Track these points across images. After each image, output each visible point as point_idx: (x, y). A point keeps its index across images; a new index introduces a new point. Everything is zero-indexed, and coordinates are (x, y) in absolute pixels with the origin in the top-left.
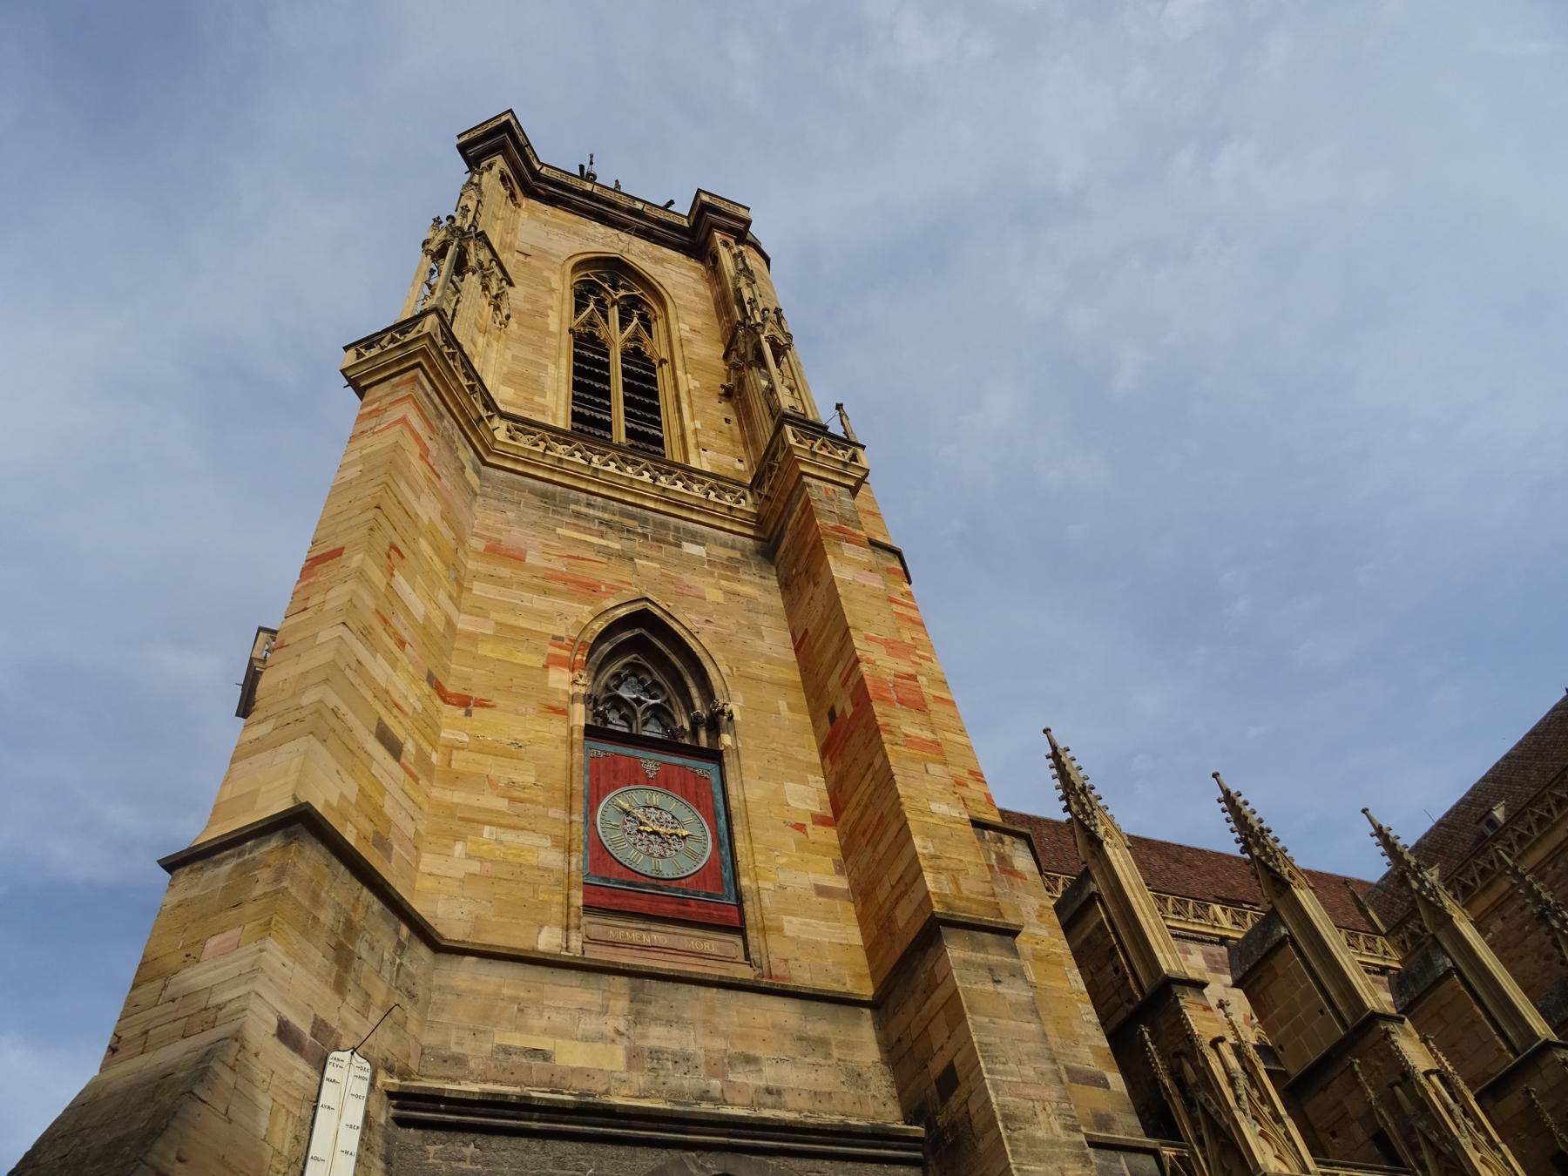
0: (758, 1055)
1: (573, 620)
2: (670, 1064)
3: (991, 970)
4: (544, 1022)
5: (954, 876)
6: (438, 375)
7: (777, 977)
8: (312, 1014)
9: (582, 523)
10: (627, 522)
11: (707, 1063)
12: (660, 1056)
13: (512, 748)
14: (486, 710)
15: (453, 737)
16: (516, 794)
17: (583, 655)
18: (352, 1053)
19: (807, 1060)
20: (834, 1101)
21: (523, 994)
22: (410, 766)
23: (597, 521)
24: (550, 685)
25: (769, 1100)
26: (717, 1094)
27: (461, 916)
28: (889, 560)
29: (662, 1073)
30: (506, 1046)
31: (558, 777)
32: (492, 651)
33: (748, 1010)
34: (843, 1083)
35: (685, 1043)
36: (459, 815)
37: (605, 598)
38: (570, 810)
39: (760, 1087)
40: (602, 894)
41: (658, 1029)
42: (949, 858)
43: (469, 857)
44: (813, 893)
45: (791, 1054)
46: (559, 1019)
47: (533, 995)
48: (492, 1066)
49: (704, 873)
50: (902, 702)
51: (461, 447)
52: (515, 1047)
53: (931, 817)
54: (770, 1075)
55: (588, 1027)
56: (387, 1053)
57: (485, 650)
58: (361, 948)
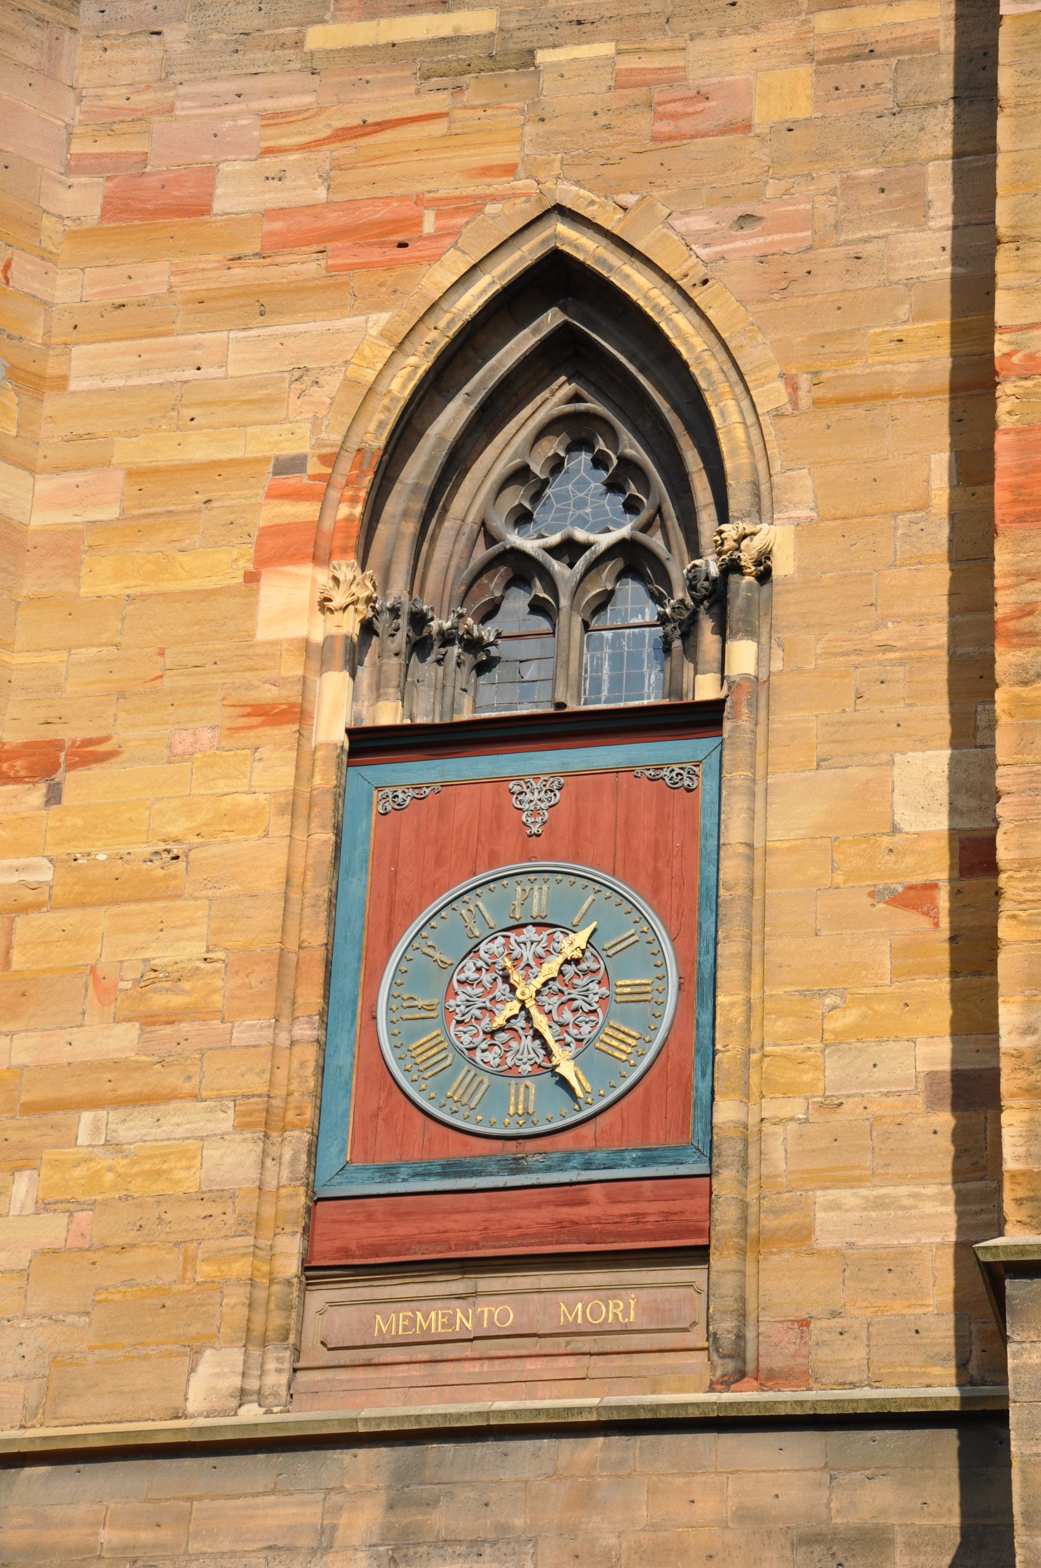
1: (333, 383)
13: (156, 869)
14: (97, 770)
15: (15, 878)
16: (161, 1001)
17: (353, 501)
24: (262, 634)
33: (680, 1481)
36: (25, 1098)
40: (370, 1217)
43: (44, 1206)
49: (647, 1091)
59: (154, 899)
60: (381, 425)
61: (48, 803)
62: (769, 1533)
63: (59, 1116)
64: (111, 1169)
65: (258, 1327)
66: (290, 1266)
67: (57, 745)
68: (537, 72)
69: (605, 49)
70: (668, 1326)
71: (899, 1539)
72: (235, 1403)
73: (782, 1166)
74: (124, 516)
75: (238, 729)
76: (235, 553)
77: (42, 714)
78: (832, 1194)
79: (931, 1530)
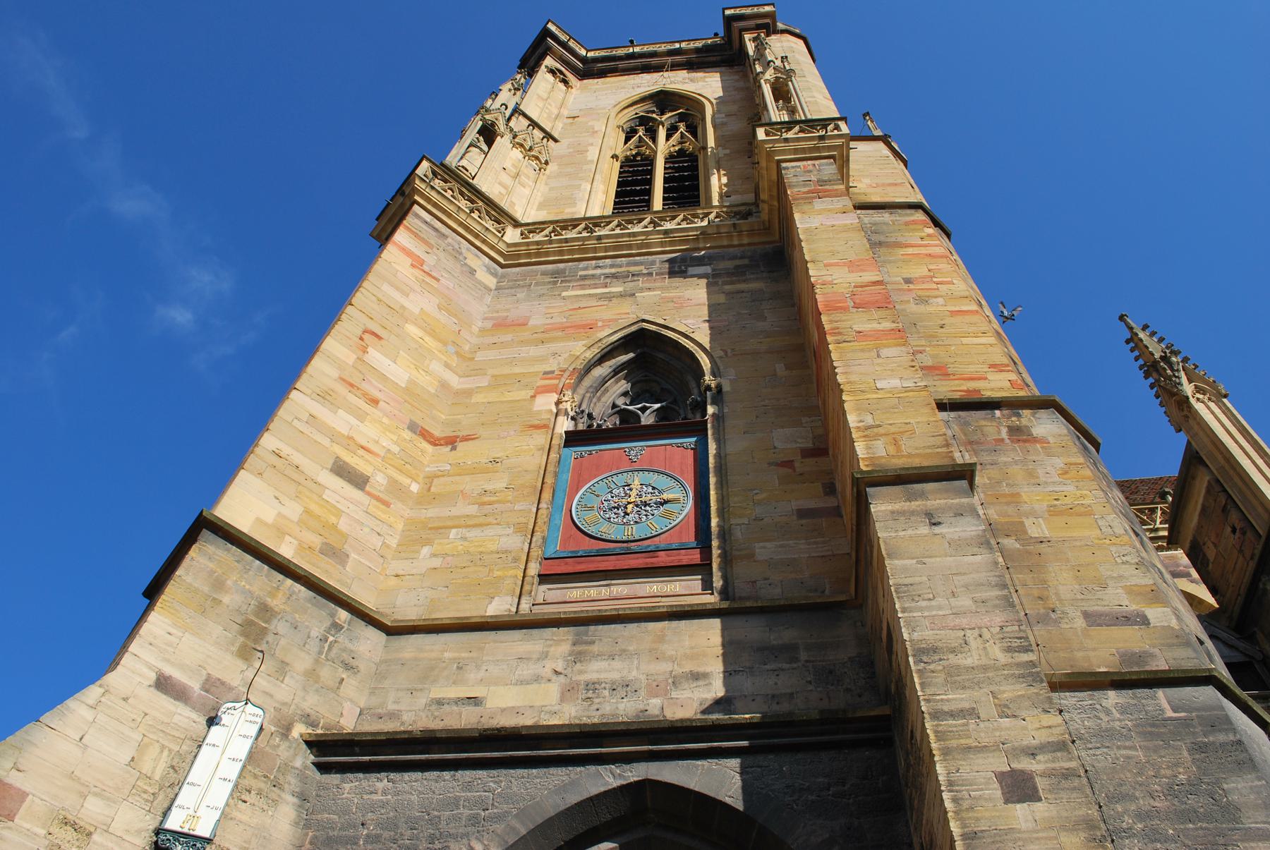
0: (708, 669)
2: (606, 693)
3: (929, 515)
4: (482, 674)
5: (894, 439)
6: (435, 205)
7: (741, 599)
8: (204, 673)
9: (587, 282)
10: (632, 269)
11: (648, 685)
12: (597, 686)
14: (470, 442)
16: (486, 499)
18: (246, 704)
19: (767, 667)
22: (382, 496)
23: (603, 277)
28: (912, 214)
34: (810, 682)
36: (430, 526)
37: (600, 331)
39: (707, 699)
41: (599, 664)
44: (795, 518)
47: (473, 654)
48: (424, 717)
49: (681, 528)
50: (856, 306)
51: (469, 256)
52: (449, 699)
55: (525, 672)
56: (308, 711)
57: (478, 398)
58: (280, 626)
60: (582, 363)
61: (451, 450)
63: (443, 531)
66: (534, 569)
67: (457, 437)
69: (660, 292)
70: (693, 592)
73: (741, 537)
74: (489, 385)
76: (528, 391)
77: (452, 429)
78: (761, 544)
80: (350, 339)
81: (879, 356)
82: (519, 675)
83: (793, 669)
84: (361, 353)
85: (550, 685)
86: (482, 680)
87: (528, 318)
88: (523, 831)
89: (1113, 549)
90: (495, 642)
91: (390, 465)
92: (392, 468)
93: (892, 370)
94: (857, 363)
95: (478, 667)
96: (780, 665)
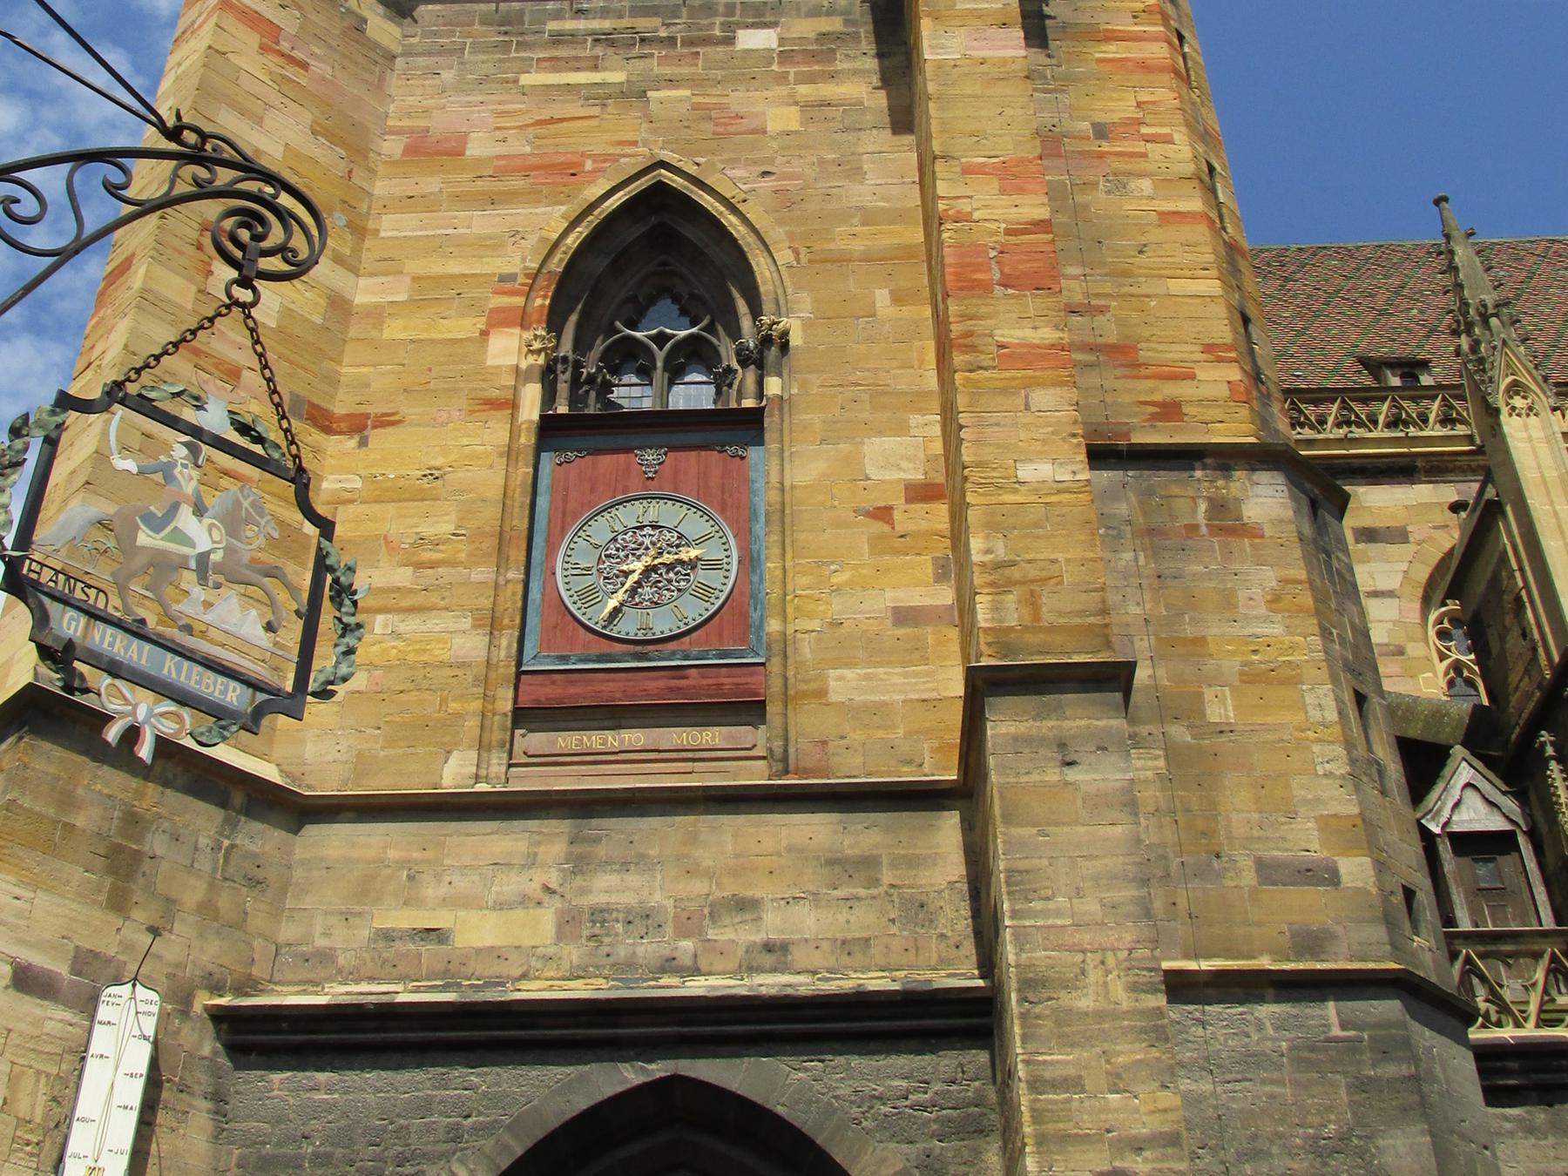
1: (533, 239)
2: (619, 927)
4: (443, 890)
11: (676, 916)
12: (606, 916)
14: (389, 429)
16: (426, 555)
17: (545, 297)
20: (873, 951)
21: (415, 855)
24: (489, 363)
25: (768, 960)
26: (687, 961)
27: (338, 756)
29: (607, 940)
30: (388, 929)
31: (489, 516)
32: (405, 329)
33: (751, 830)
34: (893, 921)
35: (646, 892)
38: (502, 562)
39: (755, 943)
41: (608, 877)
42: (1029, 562)
45: (811, 888)
46: (463, 884)
47: (429, 854)
48: (368, 959)
52: (401, 930)
53: (1015, 491)
54: (773, 924)
55: (505, 888)
59: (423, 500)
62: (807, 859)
64: (394, 647)
65: (486, 741)
66: (505, 704)
67: (367, 416)
68: (648, 101)
71: (885, 861)
72: (473, 781)
74: (411, 301)
75: (474, 411)
76: (475, 320)
77: (359, 399)
79: (903, 856)
80: (181, 253)
81: (1027, 408)
82: (497, 893)
83: (874, 898)
84: (199, 278)
85: (539, 911)
86: (444, 900)
87: (463, 139)
88: (519, 1151)
89: (1316, 748)
90: (459, 834)
91: (269, 494)
92: (276, 501)
93: (1044, 442)
94: (993, 421)
95: (438, 877)
96: (854, 891)
